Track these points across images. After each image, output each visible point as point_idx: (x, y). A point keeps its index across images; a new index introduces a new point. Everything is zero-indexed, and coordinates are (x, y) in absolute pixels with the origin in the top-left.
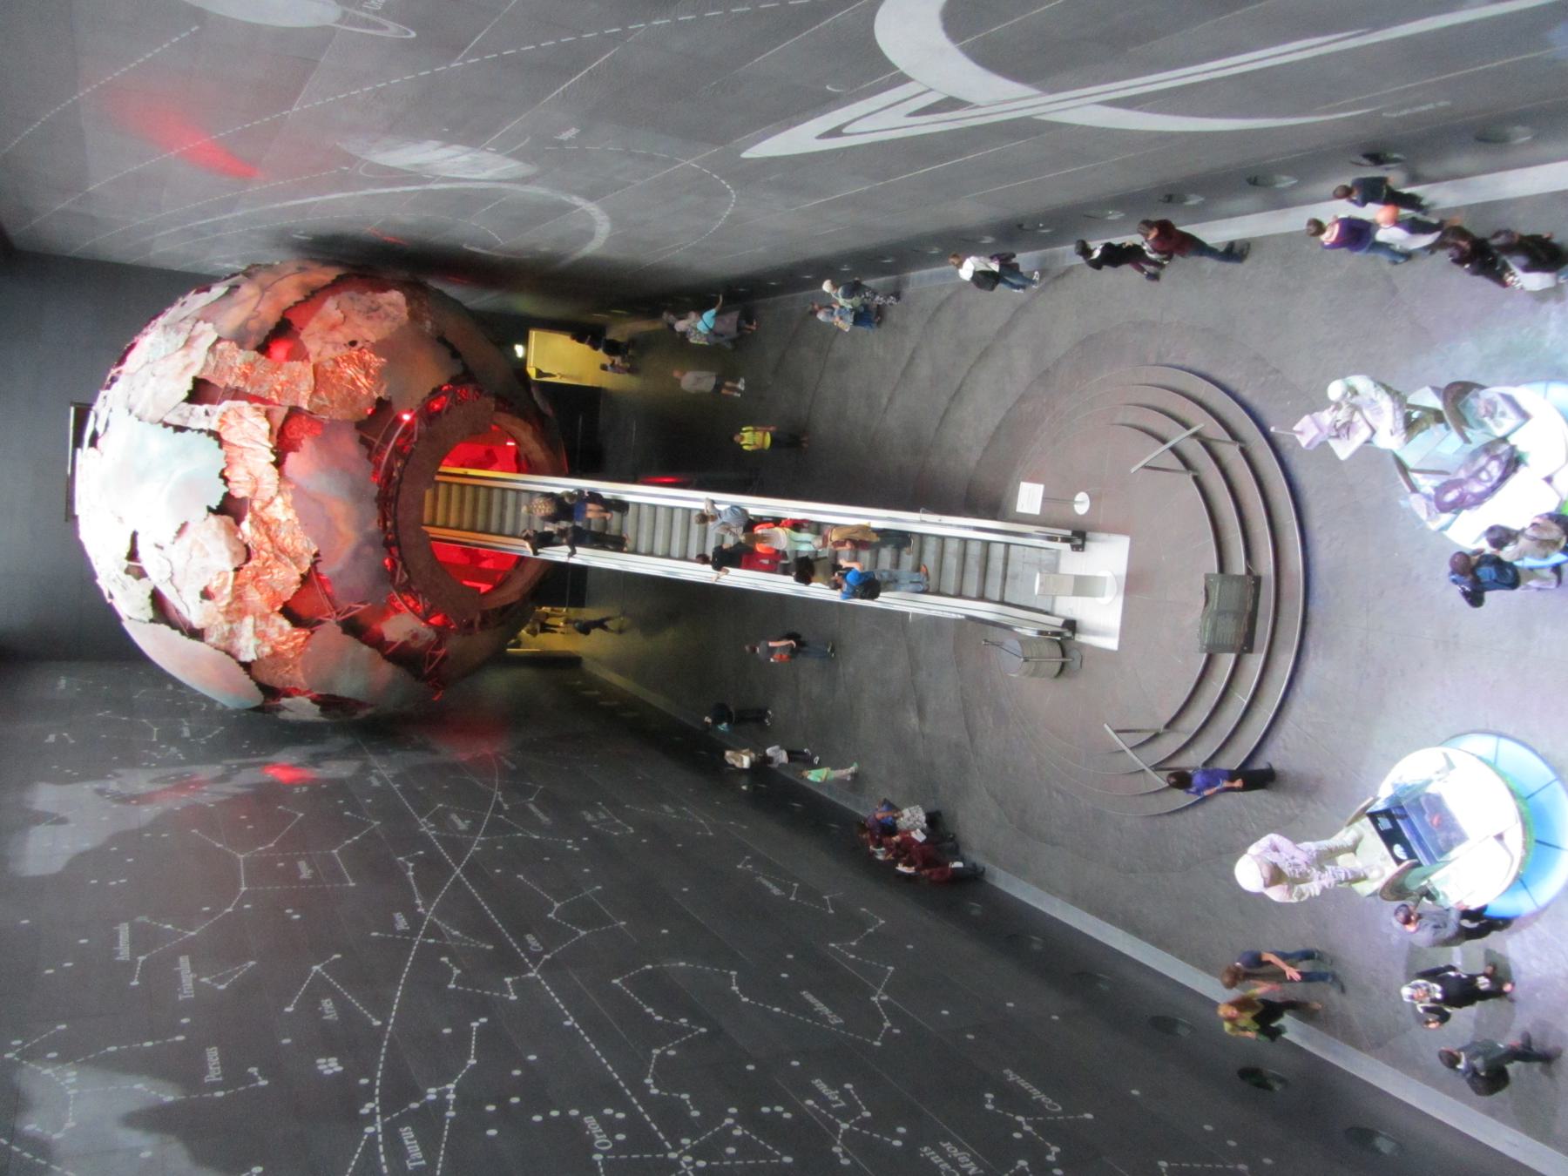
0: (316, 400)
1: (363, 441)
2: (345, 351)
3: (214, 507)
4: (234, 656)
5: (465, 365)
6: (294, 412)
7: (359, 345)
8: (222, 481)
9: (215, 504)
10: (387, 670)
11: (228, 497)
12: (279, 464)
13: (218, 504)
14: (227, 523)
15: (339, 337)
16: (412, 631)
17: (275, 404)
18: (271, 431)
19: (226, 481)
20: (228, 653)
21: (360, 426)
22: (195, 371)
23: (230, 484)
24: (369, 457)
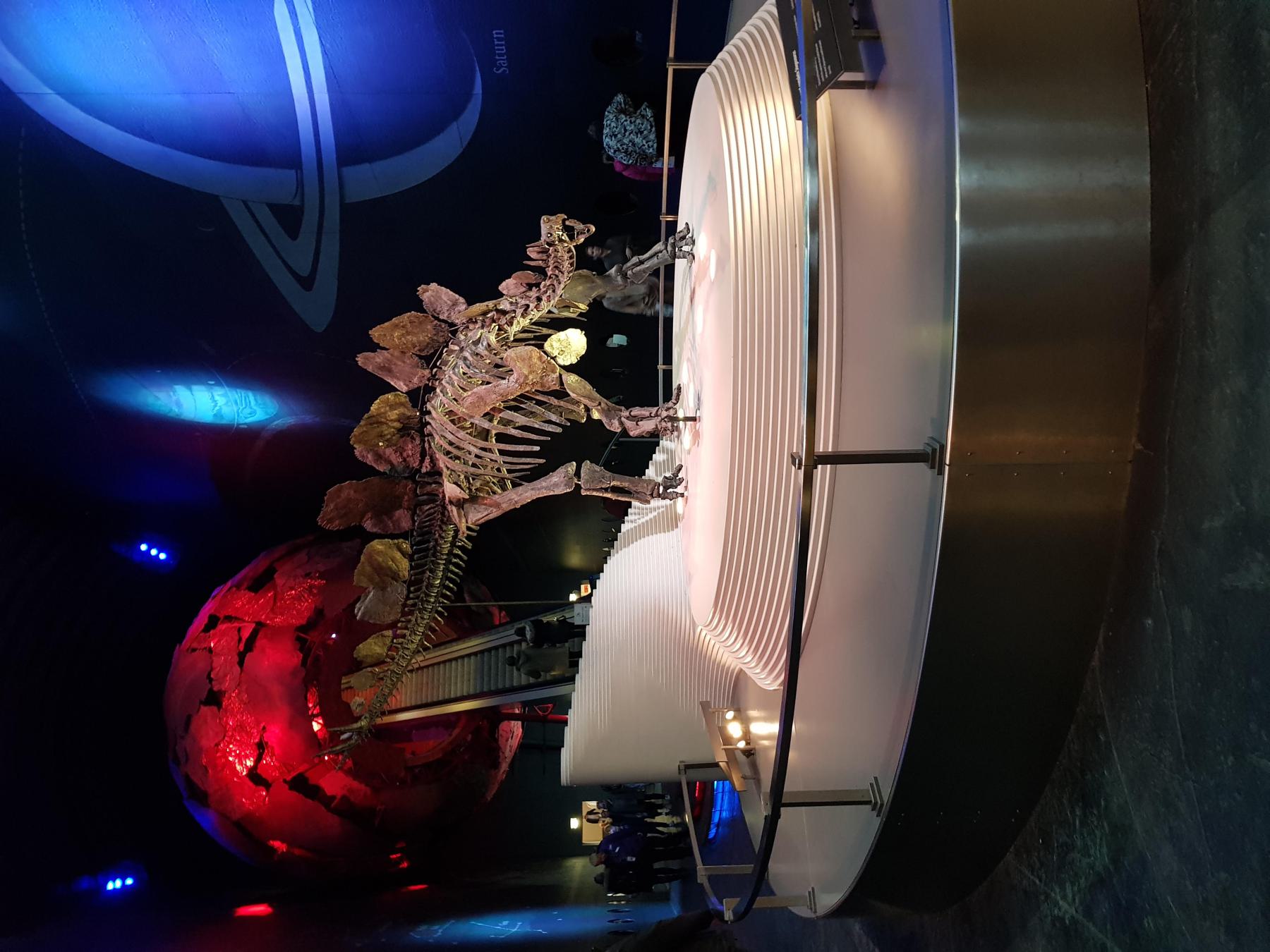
0: (271, 616)
1: (298, 639)
6: (260, 625)
7: (312, 575)
11: (211, 690)
12: (241, 663)
18: (240, 640)
19: (211, 680)
21: (301, 629)
22: (210, 613)
23: (213, 682)
24: (301, 650)
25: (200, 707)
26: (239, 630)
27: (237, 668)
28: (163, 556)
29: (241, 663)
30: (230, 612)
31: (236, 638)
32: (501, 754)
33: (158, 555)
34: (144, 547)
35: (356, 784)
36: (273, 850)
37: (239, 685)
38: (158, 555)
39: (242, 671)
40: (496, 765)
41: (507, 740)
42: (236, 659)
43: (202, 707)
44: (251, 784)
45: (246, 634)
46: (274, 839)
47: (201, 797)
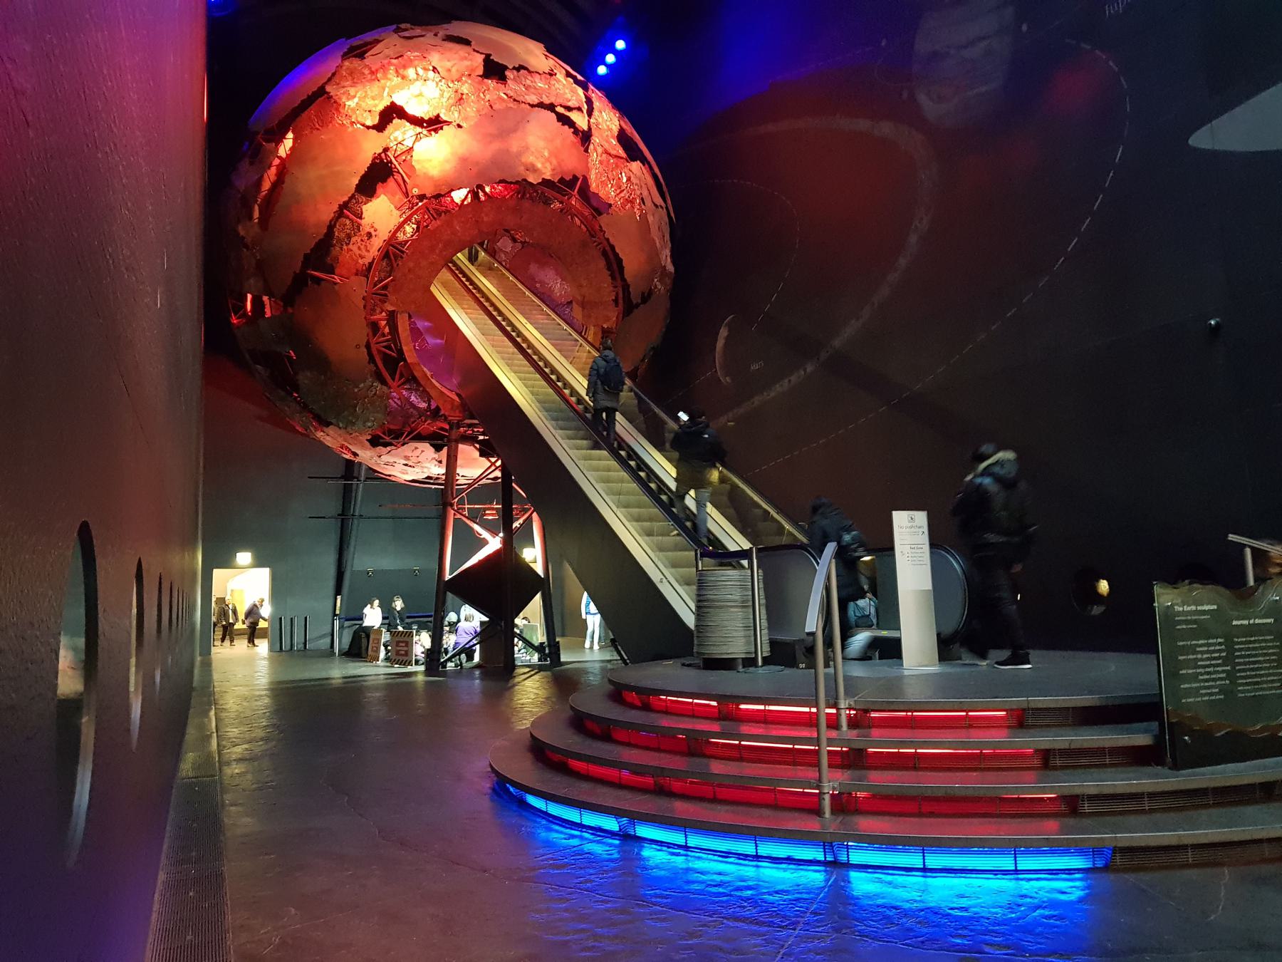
1: (575, 178)
2: (638, 193)
3: (492, 58)
4: (330, 79)
5: (637, 306)
8: (517, 66)
9: (494, 58)
10: (326, 213)
11: (506, 68)
12: (541, 105)
13: (495, 60)
14: (477, 67)
15: (645, 193)
16: (375, 231)
17: (589, 121)
18: (569, 109)
20: (334, 74)
23: (515, 72)
24: (562, 180)
25: (482, 53)
26: (579, 109)
27: (536, 101)
28: (602, 70)
29: (541, 105)
30: (596, 104)
31: (570, 104)
32: (389, 448)
33: (608, 66)
34: (620, 45)
35: (377, 243)
36: (280, 139)
37: (515, 100)
38: (604, 63)
39: (532, 106)
40: (375, 442)
41: (407, 458)
42: (547, 101)
43: (483, 56)
44: (381, 107)
45: (574, 116)
46: (295, 140)
47: (359, 53)
